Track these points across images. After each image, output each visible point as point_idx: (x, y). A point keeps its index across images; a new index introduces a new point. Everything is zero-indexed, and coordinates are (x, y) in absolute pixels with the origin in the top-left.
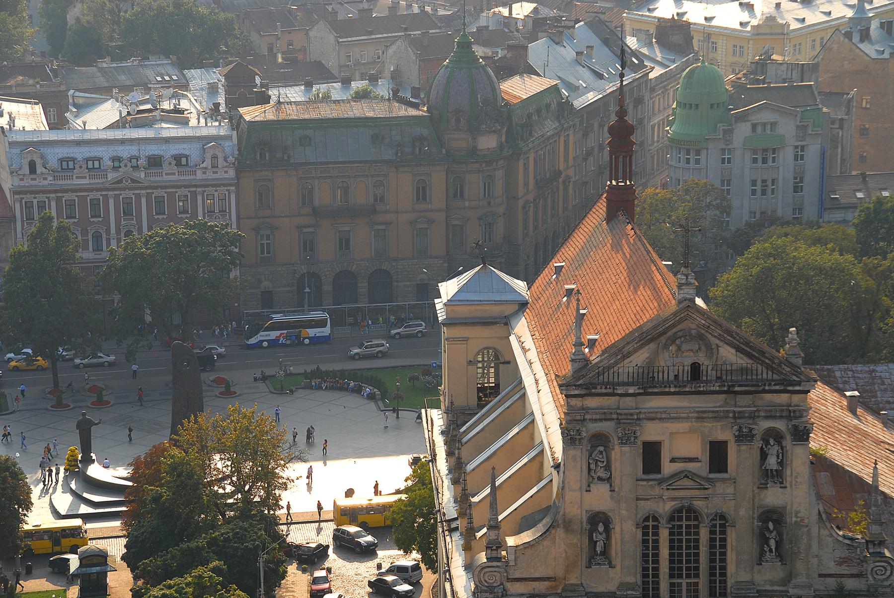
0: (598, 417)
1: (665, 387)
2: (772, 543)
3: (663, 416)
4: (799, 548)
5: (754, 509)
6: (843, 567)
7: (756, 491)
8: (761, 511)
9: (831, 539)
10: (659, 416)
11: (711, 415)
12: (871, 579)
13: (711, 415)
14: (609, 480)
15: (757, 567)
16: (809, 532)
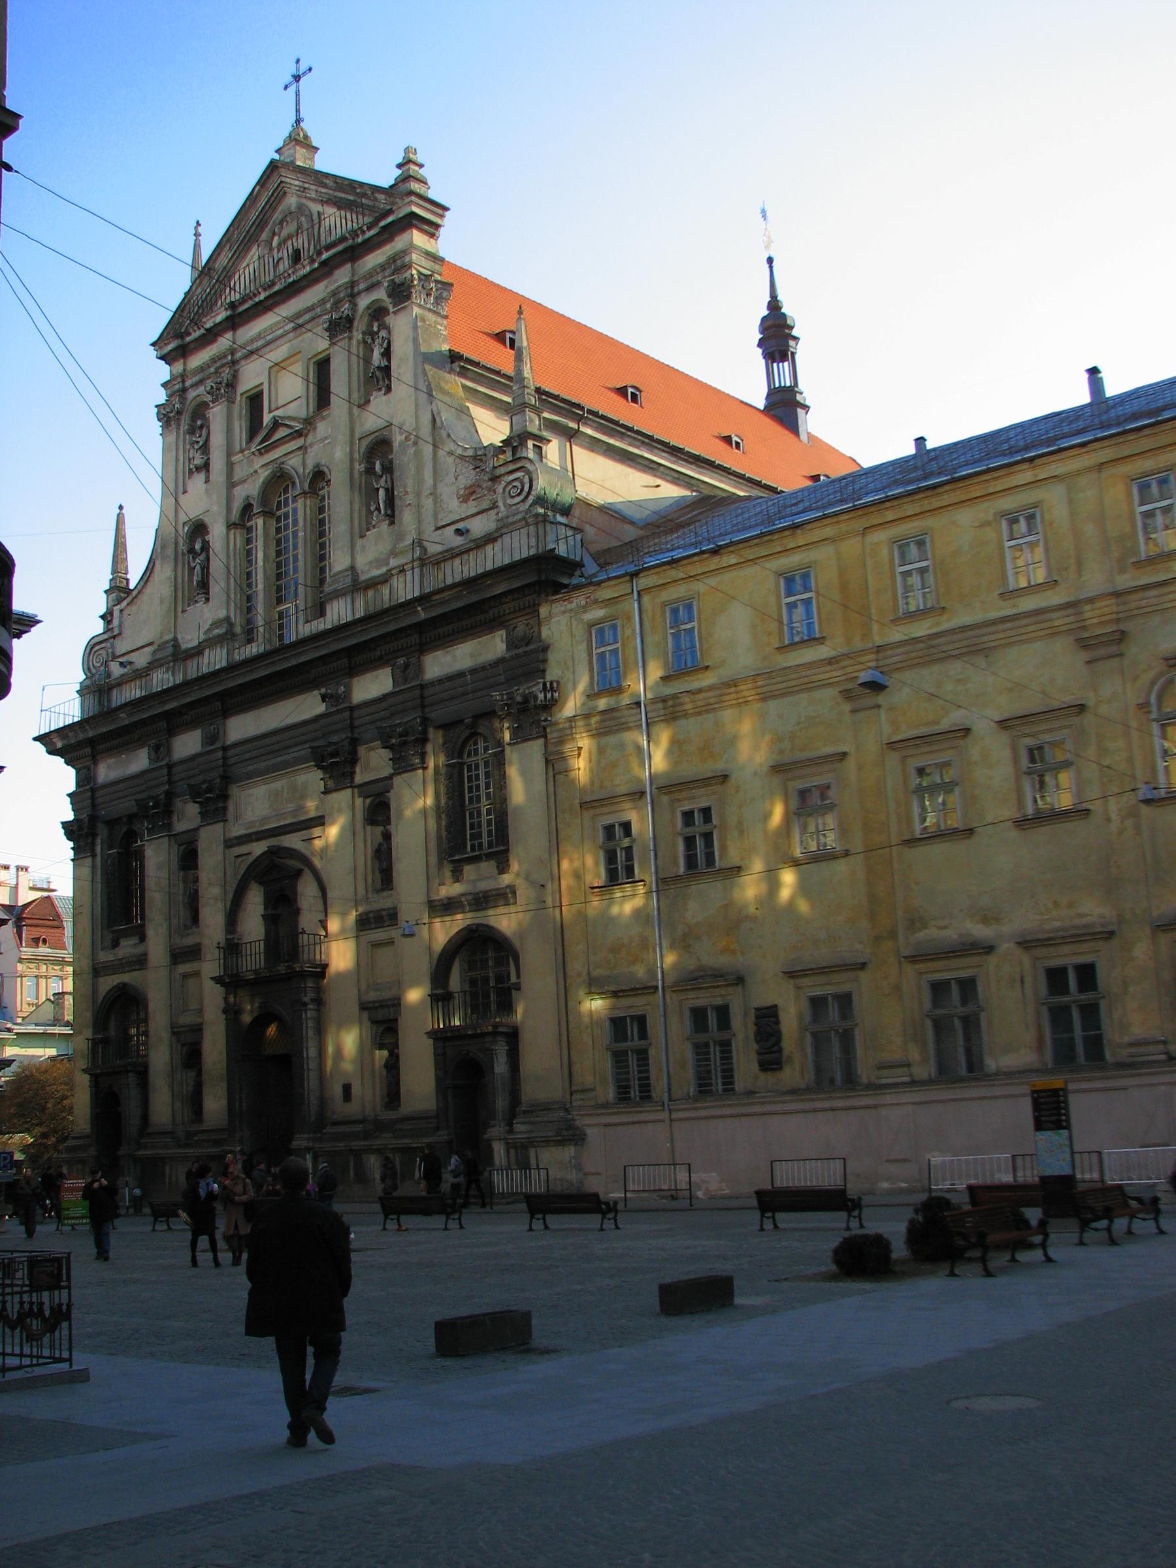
1: (255, 295)
2: (382, 493)
3: (260, 343)
4: (405, 486)
5: (352, 444)
6: (471, 503)
7: (356, 410)
8: (365, 443)
9: (450, 459)
12: (503, 508)
13: (307, 317)
14: (206, 467)
15: (359, 543)
16: (418, 454)
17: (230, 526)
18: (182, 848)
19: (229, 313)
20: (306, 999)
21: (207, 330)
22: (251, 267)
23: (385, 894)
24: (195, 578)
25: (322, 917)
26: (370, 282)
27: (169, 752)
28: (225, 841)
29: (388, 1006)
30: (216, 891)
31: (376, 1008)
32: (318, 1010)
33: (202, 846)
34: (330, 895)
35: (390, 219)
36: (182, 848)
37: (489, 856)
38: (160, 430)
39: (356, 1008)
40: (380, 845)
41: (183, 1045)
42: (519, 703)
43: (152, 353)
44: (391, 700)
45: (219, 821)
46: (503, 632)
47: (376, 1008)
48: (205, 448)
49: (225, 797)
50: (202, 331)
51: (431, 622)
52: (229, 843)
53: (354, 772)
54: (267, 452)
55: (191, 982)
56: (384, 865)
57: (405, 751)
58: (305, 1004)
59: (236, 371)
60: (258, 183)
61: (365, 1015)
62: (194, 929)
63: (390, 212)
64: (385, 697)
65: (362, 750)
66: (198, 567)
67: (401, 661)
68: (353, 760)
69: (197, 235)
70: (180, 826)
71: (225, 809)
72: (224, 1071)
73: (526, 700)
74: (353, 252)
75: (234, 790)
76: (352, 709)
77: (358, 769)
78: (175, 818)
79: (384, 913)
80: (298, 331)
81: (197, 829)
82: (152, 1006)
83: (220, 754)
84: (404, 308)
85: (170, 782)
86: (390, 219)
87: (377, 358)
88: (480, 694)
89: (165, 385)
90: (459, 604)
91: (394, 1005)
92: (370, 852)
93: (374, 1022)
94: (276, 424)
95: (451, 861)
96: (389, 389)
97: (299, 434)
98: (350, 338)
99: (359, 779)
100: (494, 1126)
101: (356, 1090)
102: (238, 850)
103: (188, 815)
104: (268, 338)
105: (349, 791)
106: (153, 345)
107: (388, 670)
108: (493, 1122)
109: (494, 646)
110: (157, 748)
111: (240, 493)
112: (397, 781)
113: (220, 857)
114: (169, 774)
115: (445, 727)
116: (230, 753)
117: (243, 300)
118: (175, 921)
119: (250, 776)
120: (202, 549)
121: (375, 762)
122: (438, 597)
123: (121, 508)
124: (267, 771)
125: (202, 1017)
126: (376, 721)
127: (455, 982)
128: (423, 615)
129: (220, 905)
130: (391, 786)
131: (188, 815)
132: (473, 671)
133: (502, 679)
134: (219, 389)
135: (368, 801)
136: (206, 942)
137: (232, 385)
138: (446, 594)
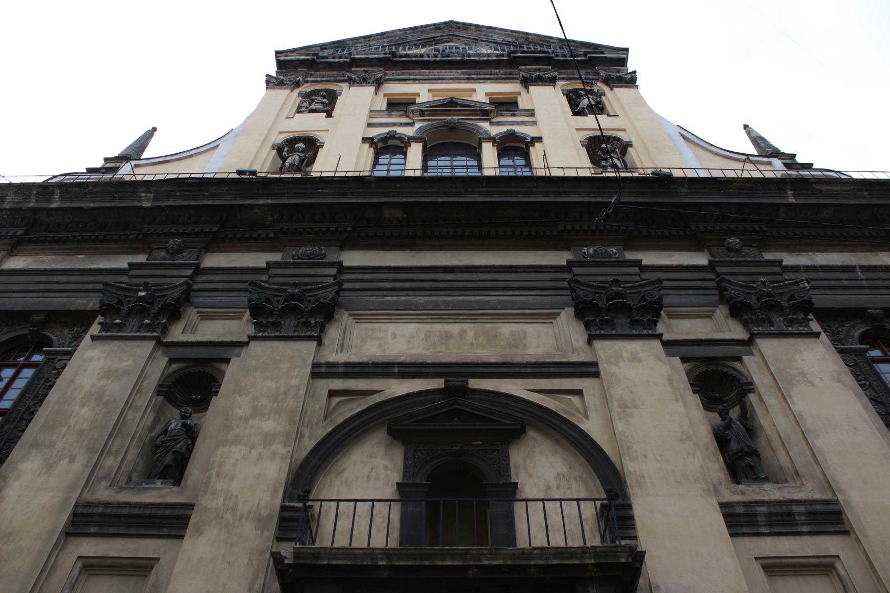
17: (365, 140)
18: (175, 366)
21: (354, 60)
27: (199, 257)
28: (315, 365)
33: (232, 371)
34: (631, 468)
36: (175, 366)
49: (327, 313)
50: (348, 60)
52: (320, 371)
54: (429, 115)
60: (434, 25)
63: (603, 53)
71: (323, 328)
75: (344, 318)
79: (795, 508)
83: (333, 271)
84: (627, 87)
102: (338, 384)
118: (111, 462)
122: (824, 187)
123: (155, 129)
124: (436, 306)
128: (793, 201)
135: (685, 365)
136: (210, 502)
138: (837, 188)
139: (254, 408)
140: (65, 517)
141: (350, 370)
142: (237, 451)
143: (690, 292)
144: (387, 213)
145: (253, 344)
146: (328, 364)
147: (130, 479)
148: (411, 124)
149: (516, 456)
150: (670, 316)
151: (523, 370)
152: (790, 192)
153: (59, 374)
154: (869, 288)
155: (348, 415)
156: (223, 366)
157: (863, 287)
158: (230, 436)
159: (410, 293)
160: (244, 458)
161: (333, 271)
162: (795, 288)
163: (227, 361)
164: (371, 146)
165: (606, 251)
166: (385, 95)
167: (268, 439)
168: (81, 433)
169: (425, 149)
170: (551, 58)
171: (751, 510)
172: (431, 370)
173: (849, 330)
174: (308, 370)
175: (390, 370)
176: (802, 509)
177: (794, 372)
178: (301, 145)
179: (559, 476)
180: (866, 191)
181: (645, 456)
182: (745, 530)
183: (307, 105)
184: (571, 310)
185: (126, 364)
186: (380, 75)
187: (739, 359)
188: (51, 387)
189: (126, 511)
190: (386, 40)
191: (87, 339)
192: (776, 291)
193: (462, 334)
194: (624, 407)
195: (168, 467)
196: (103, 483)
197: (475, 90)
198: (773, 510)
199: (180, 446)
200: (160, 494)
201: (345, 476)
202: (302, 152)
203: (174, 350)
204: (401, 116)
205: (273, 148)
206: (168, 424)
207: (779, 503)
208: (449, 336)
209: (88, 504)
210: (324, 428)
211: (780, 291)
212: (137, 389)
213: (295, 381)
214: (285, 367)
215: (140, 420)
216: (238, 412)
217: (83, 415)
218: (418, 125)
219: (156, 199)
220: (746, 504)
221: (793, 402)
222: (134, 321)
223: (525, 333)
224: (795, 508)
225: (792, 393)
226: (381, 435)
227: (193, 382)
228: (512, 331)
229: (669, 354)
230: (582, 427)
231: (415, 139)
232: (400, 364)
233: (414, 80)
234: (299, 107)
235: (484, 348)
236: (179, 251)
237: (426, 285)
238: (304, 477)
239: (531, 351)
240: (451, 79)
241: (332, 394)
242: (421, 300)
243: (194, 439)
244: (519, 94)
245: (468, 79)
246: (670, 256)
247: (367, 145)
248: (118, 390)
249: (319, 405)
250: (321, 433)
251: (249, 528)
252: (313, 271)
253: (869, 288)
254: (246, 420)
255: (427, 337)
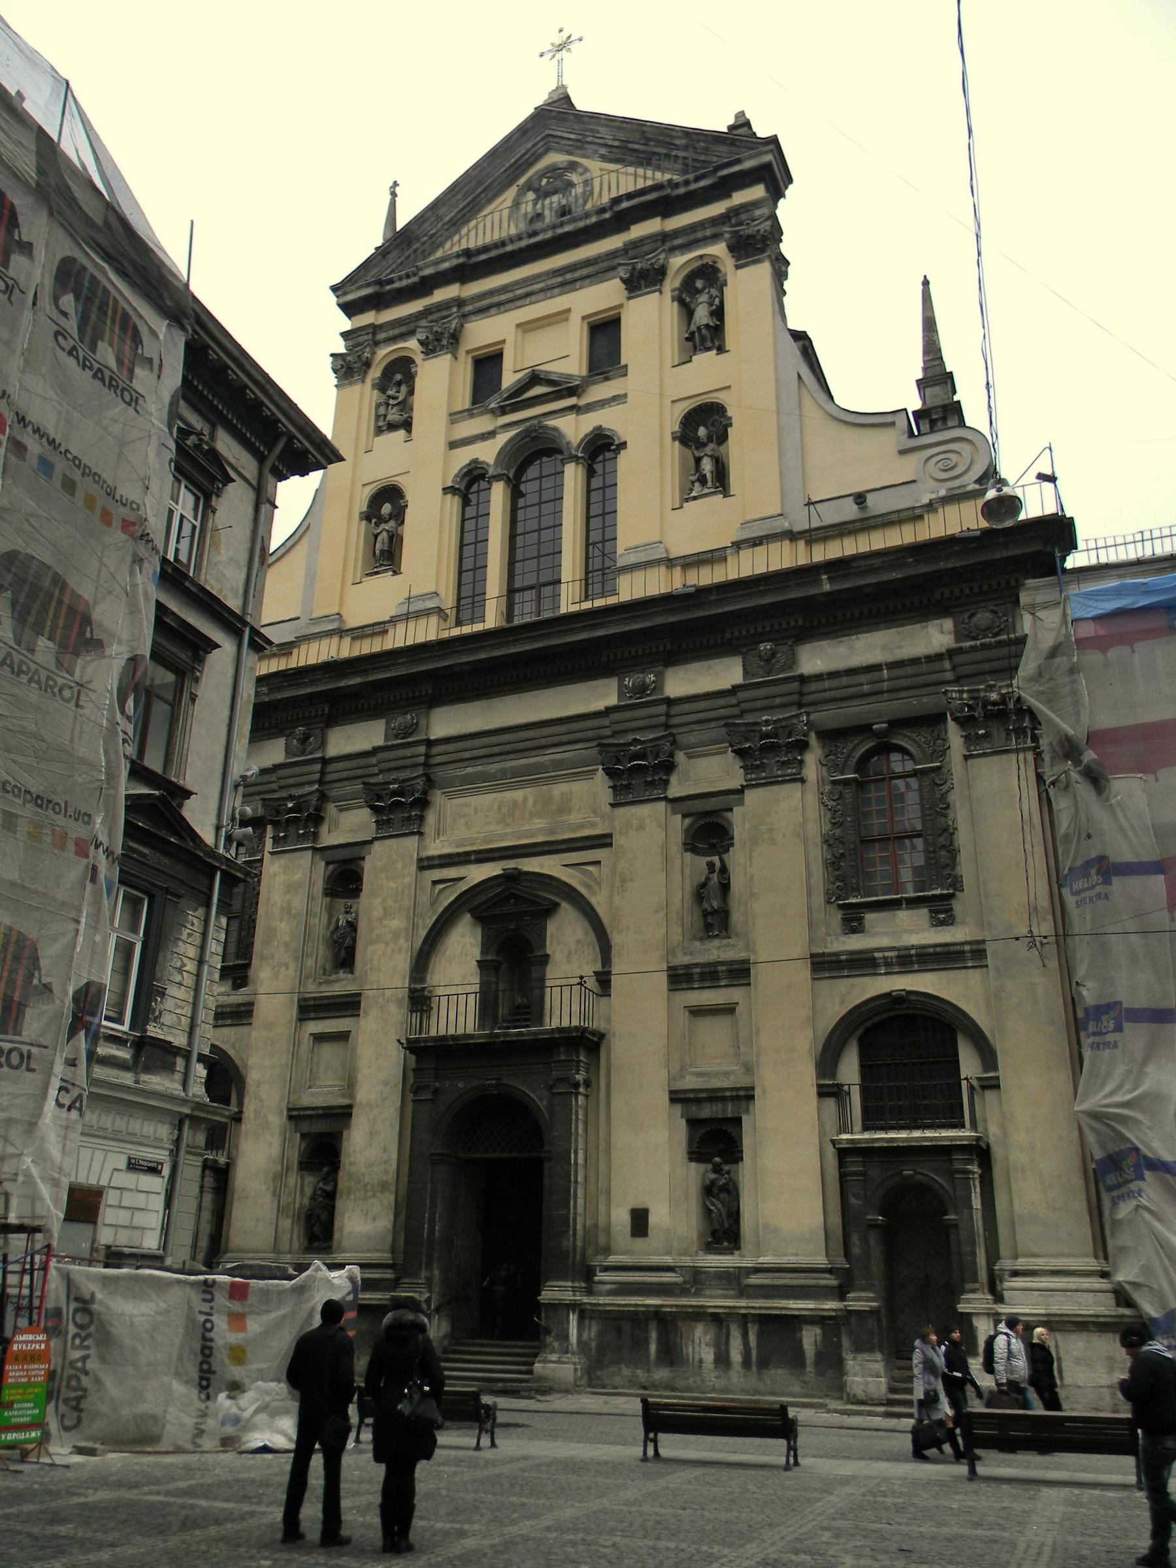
0: (397, 331)
2: (707, 466)
3: (503, 297)
10: (495, 299)
11: (585, 272)
13: (585, 272)
14: (407, 425)
18: (331, 867)
19: (461, 260)
20: (579, 1077)
21: (423, 278)
22: (497, 216)
23: (716, 942)
24: (378, 546)
25: (599, 968)
26: (692, 237)
27: (323, 745)
28: (420, 860)
29: (724, 1099)
30: (397, 923)
31: (698, 1101)
32: (587, 1096)
33: (369, 867)
34: (617, 939)
35: (736, 168)
37: (913, 903)
38: (335, 381)
39: (665, 1098)
40: (708, 879)
41: (303, 1136)
42: (994, 703)
43: (332, 299)
44: (742, 695)
45: (412, 834)
46: (948, 624)
47: (698, 1101)
48: (405, 406)
49: (423, 803)
50: (415, 279)
51: (832, 601)
52: (425, 864)
53: (667, 782)
55: (328, 1051)
56: (715, 904)
57: (767, 755)
58: (577, 1085)
59: (462, 326)
61: (678, 1108)
62: (341, 975)
63: (738, 161)
64: (735, 689)
65: (680, 757)
66: (385, 534)
67: (766, 646)
68: (669, 767)
69: (394, 195)
70: (328, 838)
71: (421, 818)
72: (391, 1177)
73: (1004, 700)
74: (664, 203)
76: (670, 702)
77: (674, 779)
78: (324, 830)
80: (568, 287)
81: (370, 842)
82: (253, 1077)
83: (422, 749)
85: (321, 782)
86: (736, 168)
87: (702, 315)
88: (903, 694)
89: (345, 335)
90: (894, 575)
91: (738, 1098)
92: (688, 888)
93: (692, 1123)
94: (535, 378)
95: (840, 906)
96: (721, 350)
97: (572, 391)
98: (661, 293)
99: (674, 791)
100: (974, 1291)
101: (658, 1217)
103: (349, 824)
104: (519, 292)
105: (661, 805)
106: (335, 289)
107: (740, 660)
108: (968, 1286)
109: (935, 636)
110: (304, 739)
111: (463, 457)
112: (751, 796)
113: (409, 880)
114: (323, 773)
115: (830, 736)
116: (436, 750)
117: (485, 249)
118: (310, 963)
119: (467, 780)
120: (391, 517)
121: (709, 771)
122: (862, 563)
125: (352, 1096)
126: (730, 717)
127: (849, 1071)
128: (827, 587)
129: (404, 943)
130: (741, 802)
131: (349, 824)
132: (892, 665)
133: (949, 676)
134: (438, 340)
135: (688, 821)
137: (455, 338)
138: (876, 562)
139: (385, 908)
140: (294, 1011)
141: (443, 861)
142: (380, 947)
143: (713, 724)
144: (457, 669)
145: (377, 844)
146: (429, 858)
147: (325, 969)
148: (491, 434)
149: (552, 927)
150: (690, 757)
151: (559, 847)
152: (824, 577)
153: (259, 881)
154: (889, 691)
155: (446, 903)
156: (362, 863)
157: (882, 692)
158: (374, 936)
159: (484, 760)
160: (384, 954)
161: (422, 749)
162: (795, 721)
163: (363, 858)
164: (454, 494)
165: (644, 682)
166: (468, 352)
167: (396, 935)
168: (287, 944)
169: (508, 481)
170: (667, 198)
171: (689, 971)
172: (497, 854)
173: (854, 748)
174: (414, 868)
175: (467, 858)
176: (724, 968)
177: (763, 828)
178: (386, 509)
179: (578, 941)
180: (911, 556)
181: (628, 928)
182: (684, 986)
183: (382, 410)
184: (601, 773)
185: (298, 876)
186: (453, 326)
187: (731, 810)
188: (258, 894)
189: (326, 1002)
190: (459, 196)
191: (267, 856)
192: (779, 725)
193: (525, 799)
194: (623, 880)
195: (344, 959)
196: (310, 981)
197: (569, 310)
198: (705, 970)
199: (348, 941)
200: (342, 985)
201: (448, 953)
202: (390, 519)
203: (328, 853)
204: (482, 413)
205: (361, 519)
206: (338, 920)
207: (709, 964)
208: (515, 804)
209: (305, 999)
210: (431, 917)
211: (784, 723)
212: (311, 897)
213: (407, 880)
214: (399, 865)
215: (320, 922)
216: (377, 913)
217: (284, 928)
218: (503, 438)
219: (271, 691)
220: (687, 967)
221: (751, 864)
222: (292, 830)
223: (571, 793)
224: (720, 968)
225: (754, 854)
226: (468, 916)
227: (345, 878)
228: (562, 793)
229: (674, 812)
230: (593, 901)
231: (497, 478)
232: (475, 852)
233: (498, 305)
234: (378, 417)
235: (540, 817)
236: (304, 739)
237: (496, 750)
238: (422, 962)
239: (573, 818)
240: (542, 290)
241: (435, 883)
242: (493, 768)
243: (356, 930)
244: (621, 306)
245: (562, 284)
246: (710, 668)
247: (449, 496)
248: (299, 902)
249: (425, 898)
250: (430, 922)
251: (393, 1008)
252: (408, 752)
253: (889, 691)
254: (381, 920)
255: (499, 809)
